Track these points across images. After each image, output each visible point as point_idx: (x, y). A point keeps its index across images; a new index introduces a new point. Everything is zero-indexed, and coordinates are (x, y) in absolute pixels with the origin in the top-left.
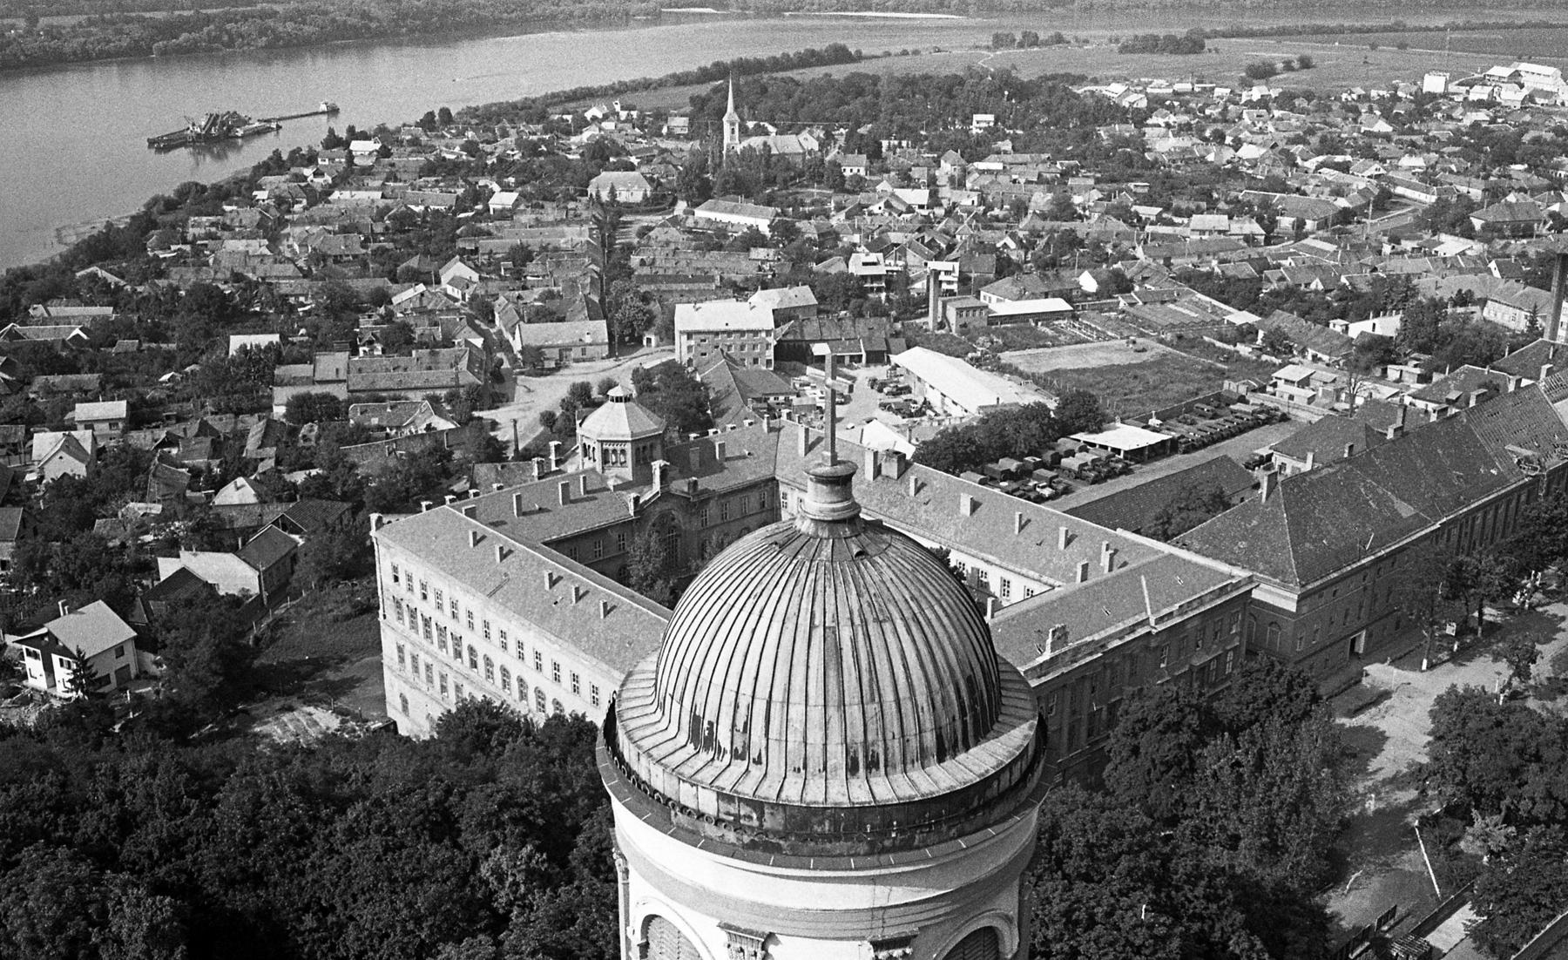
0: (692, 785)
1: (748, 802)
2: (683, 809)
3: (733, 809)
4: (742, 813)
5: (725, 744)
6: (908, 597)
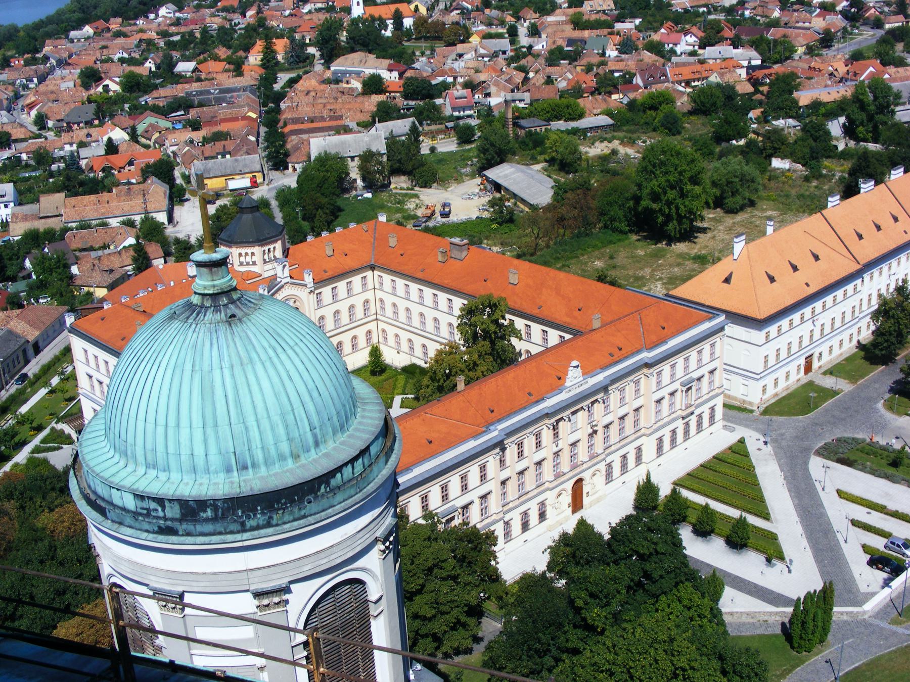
0: (118, 490)
1: (154, 499)
2: (115, 506)
3: (145, 504)
4: (151, 507)
5: (141, 459)
6: (266, 345)
